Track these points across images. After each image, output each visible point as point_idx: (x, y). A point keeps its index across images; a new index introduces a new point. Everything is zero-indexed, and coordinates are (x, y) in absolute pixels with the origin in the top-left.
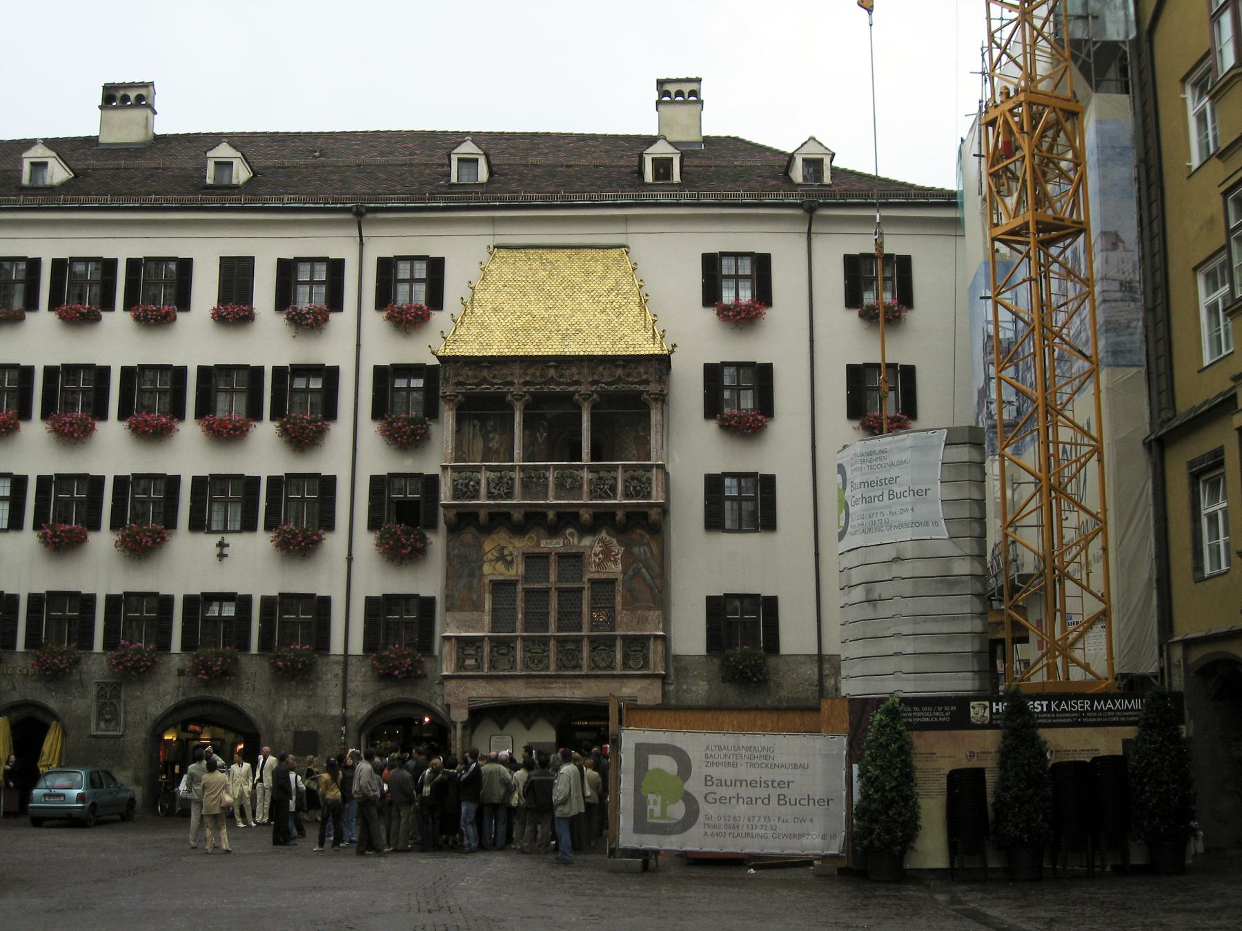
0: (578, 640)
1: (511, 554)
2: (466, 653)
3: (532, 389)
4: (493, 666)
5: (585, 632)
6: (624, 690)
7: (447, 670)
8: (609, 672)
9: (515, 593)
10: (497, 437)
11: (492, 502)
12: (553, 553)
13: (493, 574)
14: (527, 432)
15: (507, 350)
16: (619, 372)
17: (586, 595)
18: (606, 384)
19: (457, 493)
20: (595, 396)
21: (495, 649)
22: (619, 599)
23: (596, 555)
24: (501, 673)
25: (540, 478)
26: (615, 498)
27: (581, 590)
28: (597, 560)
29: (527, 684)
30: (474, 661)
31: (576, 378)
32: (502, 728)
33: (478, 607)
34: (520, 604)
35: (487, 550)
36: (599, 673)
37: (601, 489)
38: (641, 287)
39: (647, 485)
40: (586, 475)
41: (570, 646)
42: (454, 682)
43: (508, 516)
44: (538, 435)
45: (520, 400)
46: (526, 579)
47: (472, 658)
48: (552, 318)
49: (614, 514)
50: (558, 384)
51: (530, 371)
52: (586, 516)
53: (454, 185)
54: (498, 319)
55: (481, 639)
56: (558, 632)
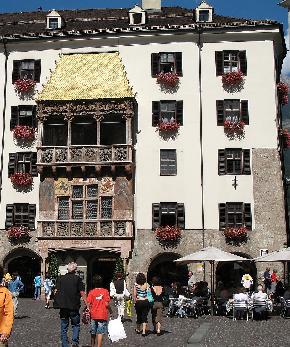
1: (67, 186)
3: (75, 114)
4: (58, 234)
6: (115, 244)
8: (108, 237)
11: (58, 163)
12: (85, 185)
14: (75, 133)
15: (64, 98)
18: (107, 111)
19: (44, 159)
22: (113, 204)
23: (103, 186)
24: (62, 237)
25: (78, 152)
27: (96, 201)
28: (104, 188)
31: (94, 108)
33: (52, 208)
34: (70, 207)
35: (56, 184)
36: (104, 237)
37: (105, 157)
38: (123, 68)
39: (124, 154)
41: (92, 225)
44: (80, 134)
46: (74, 196)
47: (49, 231)
48: (85, 84)
49: (110, 167)
50: (86, 111)
52: (98, 168)
53: (48, 30)
54: (62, 85)
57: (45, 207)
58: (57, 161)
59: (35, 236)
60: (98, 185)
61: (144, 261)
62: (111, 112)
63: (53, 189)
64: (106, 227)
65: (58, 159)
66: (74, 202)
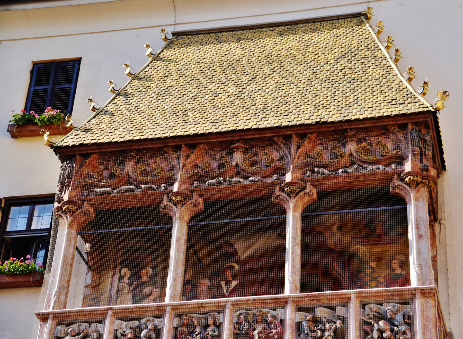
10: (156, 291)
20: (309, 188)
25: (207, 326)
44: (223, 284)
62: (345, 172)
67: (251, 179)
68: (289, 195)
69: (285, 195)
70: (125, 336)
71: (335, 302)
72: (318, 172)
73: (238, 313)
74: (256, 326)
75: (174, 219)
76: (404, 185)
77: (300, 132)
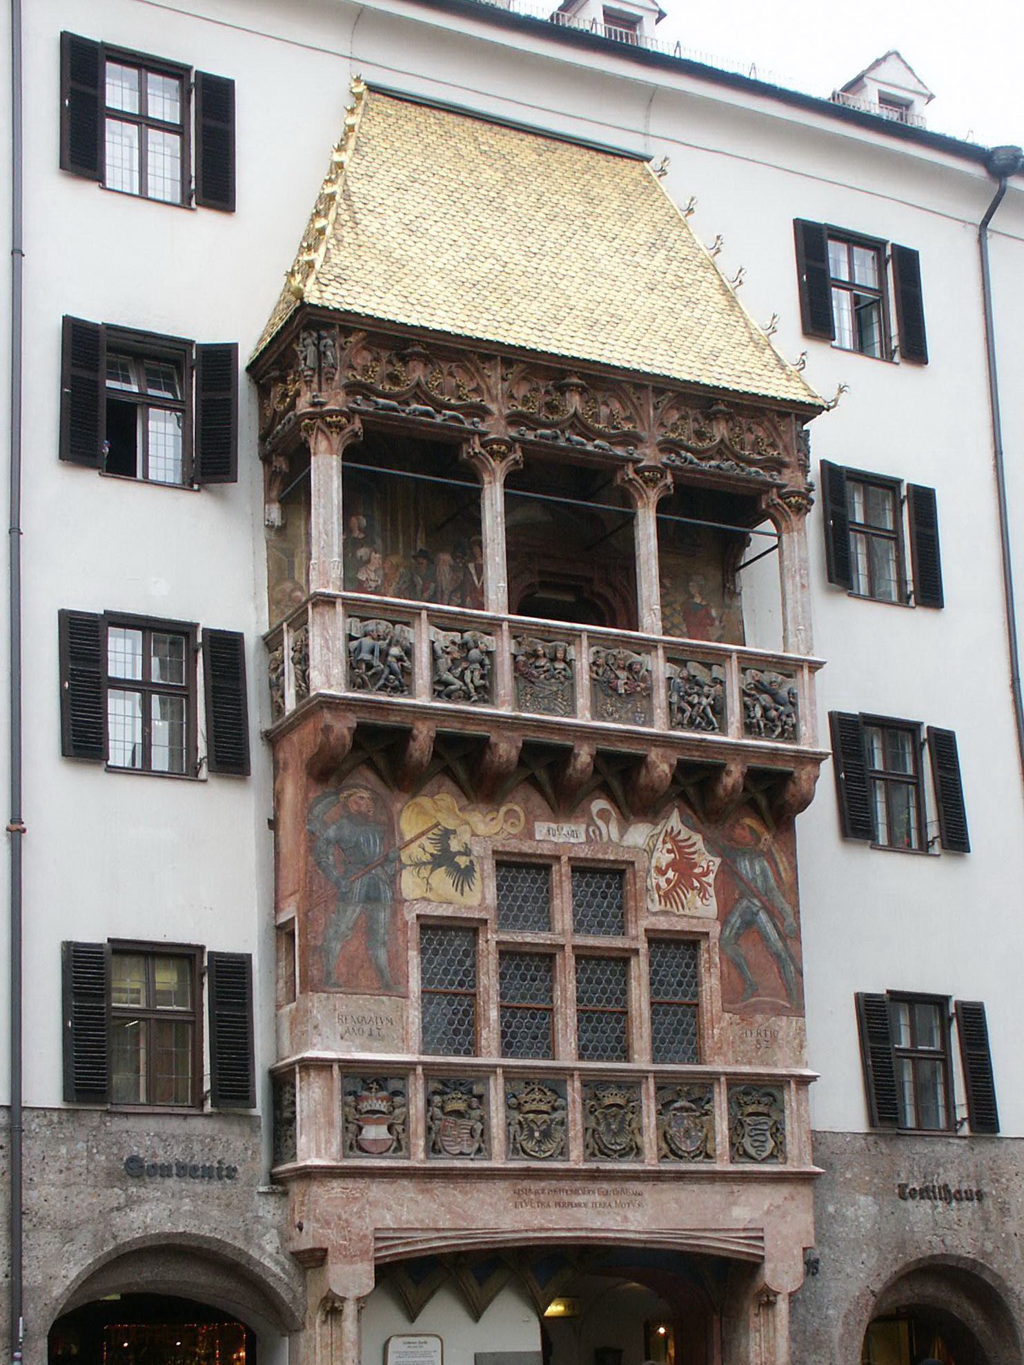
0: (631, 1083)
1: (467, 852)
2: (365, 1106)
3: (530, 436)
4: (433, 1149)
5: (642, 1060)
7: (318, 1155)
8: (703, 1167)
9: (471, 952)
12: (564, 859)
13: (424, 899)
16: (720, 431)
17: (640, 970)
21: (437, 1099)
22: (711, 985)
23: (662, 872)
24: (458, 1164)
25: (553, 659)
26: (723, 730)
27: (623, 959)
28: (663, 885)
29: (517, 1193)
30: (384, 1128)
32: (412, 1314)
33: (391, 985)
35: (407, 838)
36: (684, 1166)
37: (692, 706)
39: (789, 708)
40: (659, 667)
42: (336, 1187)
43: (483, 744)
45: (503, 456)
47: (378, 1122)
49: (717, 770)
50: (591, 434)
51: (522, 390)
55: (411, 1066)
56: (581, 1057)
57: (344, 970)
58: (437, 694)
59: (253, 1159)
60: (633, 863)
61: (846, 1305)
62: (718, 467)
63: (391, 863)
64: (687, 1110)
65: (447, 684)
66: (507, 953)
67: (597, 442)
68: (645, 482)
69: (640, 481)
70: (448, 653)
71: (709, 660)
72: (686, 459)
73: (594, 649)
74: (618, 672)
75: (486, 478)
76: (785, 506)
77: (661, 385)
